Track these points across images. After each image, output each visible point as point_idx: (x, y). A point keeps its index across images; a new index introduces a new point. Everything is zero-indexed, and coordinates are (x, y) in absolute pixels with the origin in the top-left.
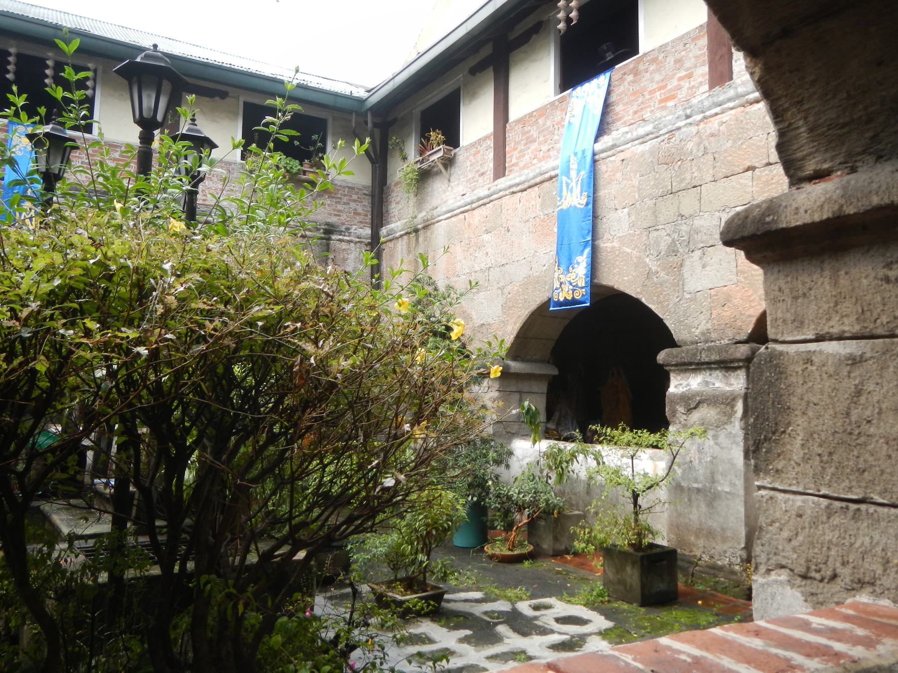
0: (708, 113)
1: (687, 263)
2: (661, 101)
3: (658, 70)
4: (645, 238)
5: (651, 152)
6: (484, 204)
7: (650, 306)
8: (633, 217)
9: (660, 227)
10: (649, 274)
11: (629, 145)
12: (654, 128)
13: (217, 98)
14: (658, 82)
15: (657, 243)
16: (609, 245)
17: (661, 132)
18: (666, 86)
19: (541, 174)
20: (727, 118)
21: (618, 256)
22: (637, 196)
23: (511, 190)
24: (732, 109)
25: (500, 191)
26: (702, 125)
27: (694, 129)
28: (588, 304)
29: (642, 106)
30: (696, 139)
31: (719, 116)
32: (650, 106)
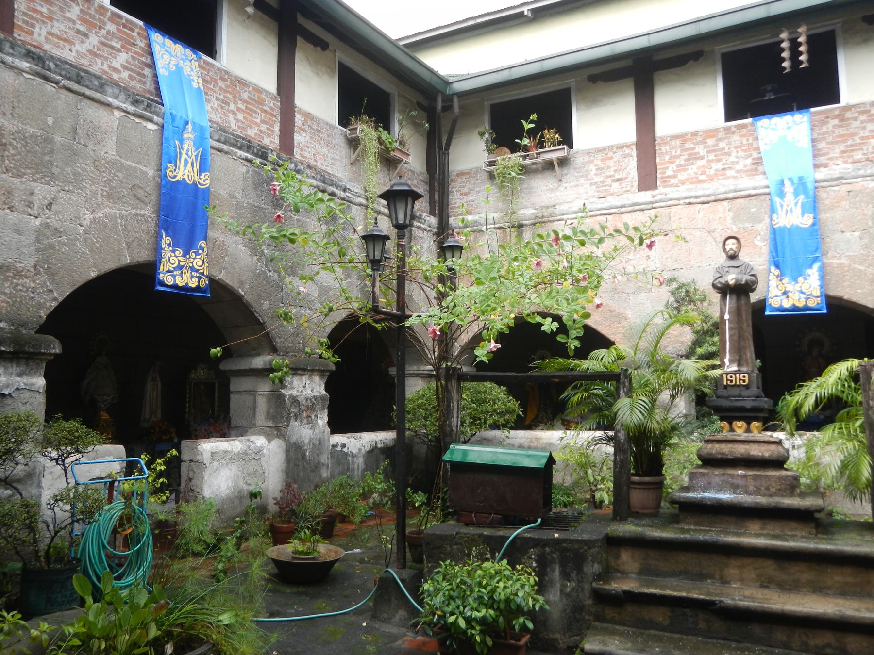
6: (642, 210)
8: (866, 241)
11: (860, 179)
13: (319, 48)
16: (835, 261)
19: (735, 191)
21: (848, 271)
23: (688, 201)
25: (671, 200)
28: (825, 311)
29: (851, 148)
32: (862, 149)
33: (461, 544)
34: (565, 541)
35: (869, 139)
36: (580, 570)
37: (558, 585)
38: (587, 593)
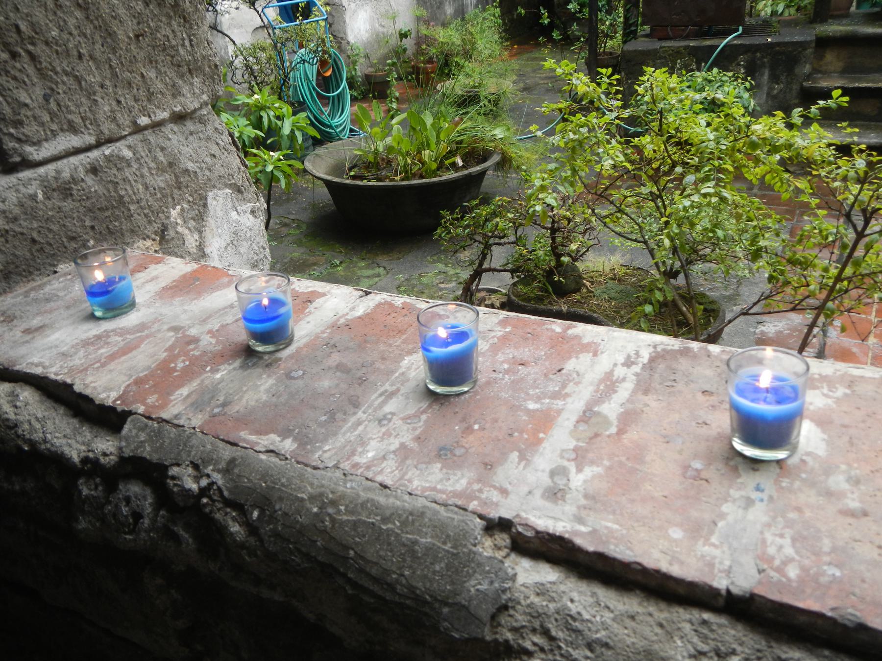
33: (665, 57)
34: (778, 44)
36: (790, 71)
37: (765, 89)
38: (794, 93)
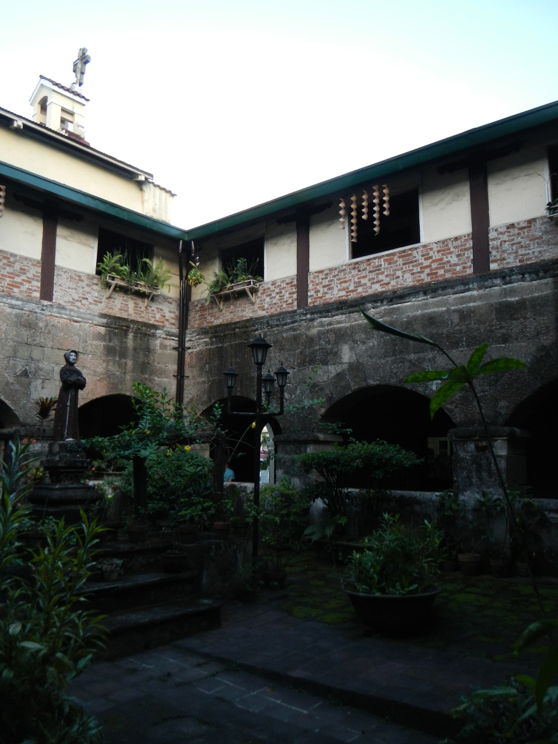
0: (54, 314)
1: (33, 384)
2: (9, 284)
3: (10, 266)
4: (6, 362)
5: (17, 316)
7: (7, 401)
9: (18, 359)
10: (7, 384)
12: (22, 304)
14: (8, 272)
15: (15, 367)
17: (25, 309)
18: (13, 278)
20: (62, 322)
22: (3, 336)
24: (65, 319)
26: (48, 318)
27: (44, 317)
30: (45, 323)
31: (57, 318)
35: (6, 277)
